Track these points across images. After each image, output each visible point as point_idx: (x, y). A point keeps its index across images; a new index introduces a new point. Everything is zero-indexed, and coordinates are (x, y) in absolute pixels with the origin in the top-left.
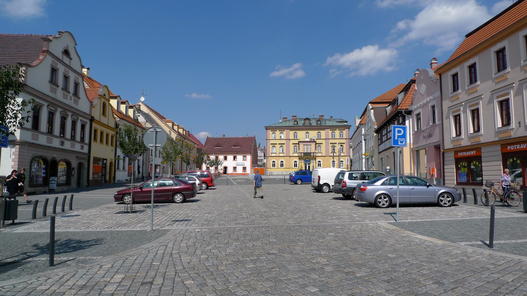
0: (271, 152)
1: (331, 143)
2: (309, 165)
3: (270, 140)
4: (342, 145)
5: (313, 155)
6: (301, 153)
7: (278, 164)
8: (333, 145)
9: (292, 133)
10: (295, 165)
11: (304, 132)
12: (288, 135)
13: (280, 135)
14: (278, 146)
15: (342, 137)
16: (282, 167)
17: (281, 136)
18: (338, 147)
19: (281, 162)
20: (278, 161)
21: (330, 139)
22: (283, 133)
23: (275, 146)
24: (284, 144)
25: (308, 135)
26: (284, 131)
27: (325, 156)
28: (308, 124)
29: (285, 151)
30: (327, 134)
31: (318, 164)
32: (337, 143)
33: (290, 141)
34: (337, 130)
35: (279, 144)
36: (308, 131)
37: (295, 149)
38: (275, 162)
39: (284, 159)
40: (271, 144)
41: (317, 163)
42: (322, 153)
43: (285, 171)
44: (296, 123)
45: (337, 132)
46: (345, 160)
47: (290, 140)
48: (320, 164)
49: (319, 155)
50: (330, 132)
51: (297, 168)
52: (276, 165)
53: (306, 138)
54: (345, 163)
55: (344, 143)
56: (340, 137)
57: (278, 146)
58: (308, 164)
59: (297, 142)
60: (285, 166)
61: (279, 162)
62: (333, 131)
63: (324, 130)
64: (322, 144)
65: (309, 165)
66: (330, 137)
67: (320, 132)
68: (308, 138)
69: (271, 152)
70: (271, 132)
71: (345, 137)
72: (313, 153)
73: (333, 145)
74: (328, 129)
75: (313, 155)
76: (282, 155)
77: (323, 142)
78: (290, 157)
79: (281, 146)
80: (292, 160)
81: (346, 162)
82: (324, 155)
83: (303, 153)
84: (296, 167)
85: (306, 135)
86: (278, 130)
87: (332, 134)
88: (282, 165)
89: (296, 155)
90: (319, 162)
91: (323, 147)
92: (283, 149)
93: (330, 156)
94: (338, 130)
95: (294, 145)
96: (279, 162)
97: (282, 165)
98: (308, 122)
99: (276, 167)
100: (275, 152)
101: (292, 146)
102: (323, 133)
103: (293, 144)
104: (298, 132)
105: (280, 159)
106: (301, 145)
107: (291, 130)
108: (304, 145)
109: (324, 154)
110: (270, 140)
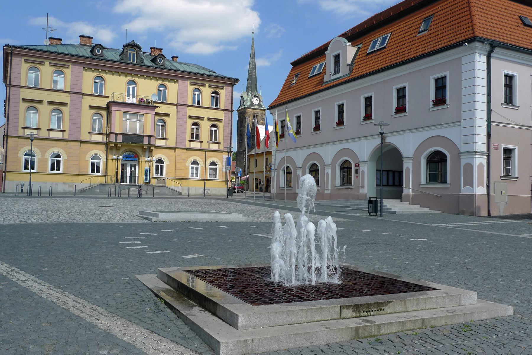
0: (21, 125)
1: (191, 117)
2: (133, 169)
3: (21, 87)
4: (214, 123)
5: (149, 142)
6: (116, 134)
7: (43, 160)
8: (196, 122)
9: (89, 76)
10: (95, 168)
11: (124, 79)
12: (77, 80)
13: (55, 78)
14: (45, 109)
15: (217, 105)
16: (55, 172)
17: (56, 82)
18: (205, 127)
19: (157, 162)
20: (43, 153)
21: (188, 106)
22: (62, 73)
23: (36, 109)
24: (65, 104)
25: (134, 89)
26: (67, 67)
27: (175, 149)
28: (134, 60)
29: (66, 125)
30: (181, 93)
31: (157, 167)
32: (206, 119)
33: (82, 98)
34: (207, 85)
35: (50, 103)
36: (136, 79)
37: (94, 121)
38: (60, 157)
39: (63, 148)
40: (25, 100)
41: (155, 164)
42: (167, 139)
43: (64, 183)
44: (99, 52)
45: (207, 91)
46: (221, 160)
47: (83, 94)
48: (162, 167)
49: (159, 143)
50: (191, 89)
51: (100, 174)
52: (64, 165)
53: (129, 96)
54: (221, 169)
55: (220, 120)
56: (212, 104)
57: (45, 109)
58: (131, 166)
59: (103, 103)
60: (38, 167)
61: (46, 157)
62: (198, 87)
63: (175, 82)
64: (168, 115)
65: (133, 169)
66: (190, 102)
67: (165, 86)
68: (133, 96)
69: (21, 125)
70: (25, 66)
71: (222, 104)
72: (150, 137)
73: (196, 122)
74: (186, 79)
75: (149, 142)
76: (58, 135)
77: (171, 110)
78: (81, 142)
79: (54, 111)
80: (188, 158)
81: (222, 165)
82: (173, 145)
83: (122, 134)
84: (98, 171)
85: (129, 88)
86: (47, 63)
87: (194, 95)
88: (56, 166)
89: (99, 138)
90: (160, 161)
91: (171, 122)
92: (59, 119)
93: (188, 149)
94: (210, 87)
95: (94, 111)
96: (46, 157)
97: (56, 166)
98: (134, 54)
99: (35, 171)
100: (36, 126)
101: (87, 114)
102: (172, 88)
103: (91, 107)
104: (108, 77)
105: (53, 147)
106: (117, 113)
107: (88, 67)
108: (125, 113)
109: (172, 143)
110: (21, 87)
